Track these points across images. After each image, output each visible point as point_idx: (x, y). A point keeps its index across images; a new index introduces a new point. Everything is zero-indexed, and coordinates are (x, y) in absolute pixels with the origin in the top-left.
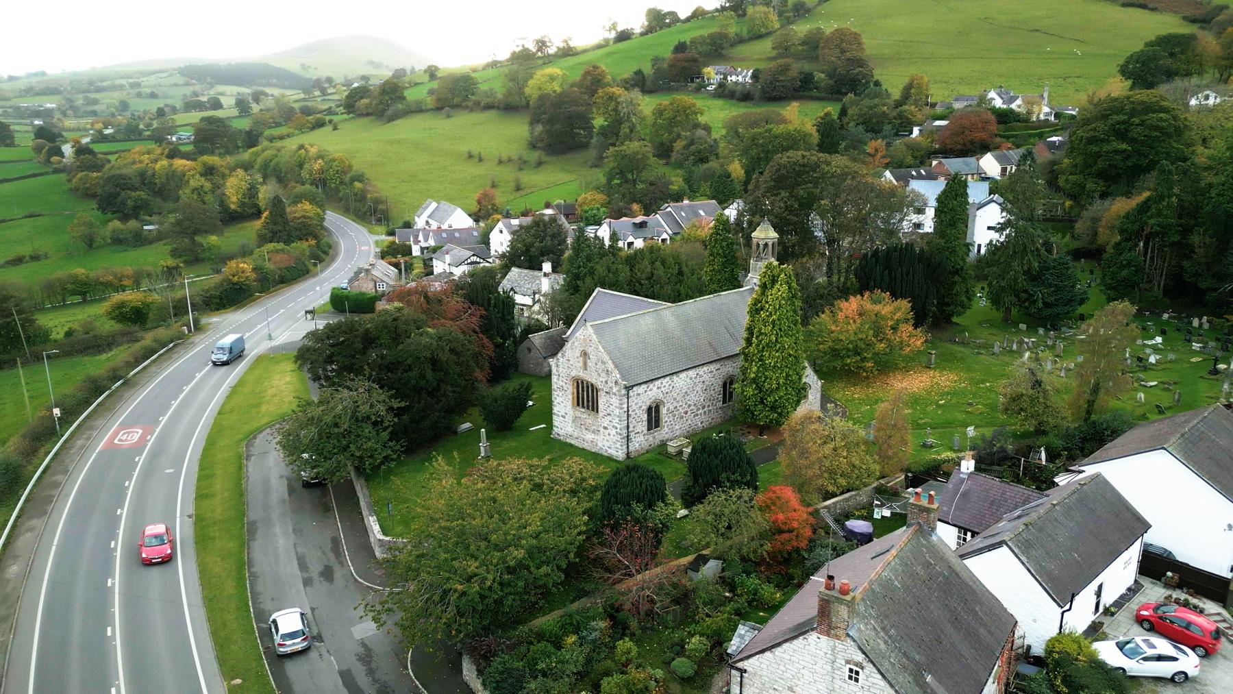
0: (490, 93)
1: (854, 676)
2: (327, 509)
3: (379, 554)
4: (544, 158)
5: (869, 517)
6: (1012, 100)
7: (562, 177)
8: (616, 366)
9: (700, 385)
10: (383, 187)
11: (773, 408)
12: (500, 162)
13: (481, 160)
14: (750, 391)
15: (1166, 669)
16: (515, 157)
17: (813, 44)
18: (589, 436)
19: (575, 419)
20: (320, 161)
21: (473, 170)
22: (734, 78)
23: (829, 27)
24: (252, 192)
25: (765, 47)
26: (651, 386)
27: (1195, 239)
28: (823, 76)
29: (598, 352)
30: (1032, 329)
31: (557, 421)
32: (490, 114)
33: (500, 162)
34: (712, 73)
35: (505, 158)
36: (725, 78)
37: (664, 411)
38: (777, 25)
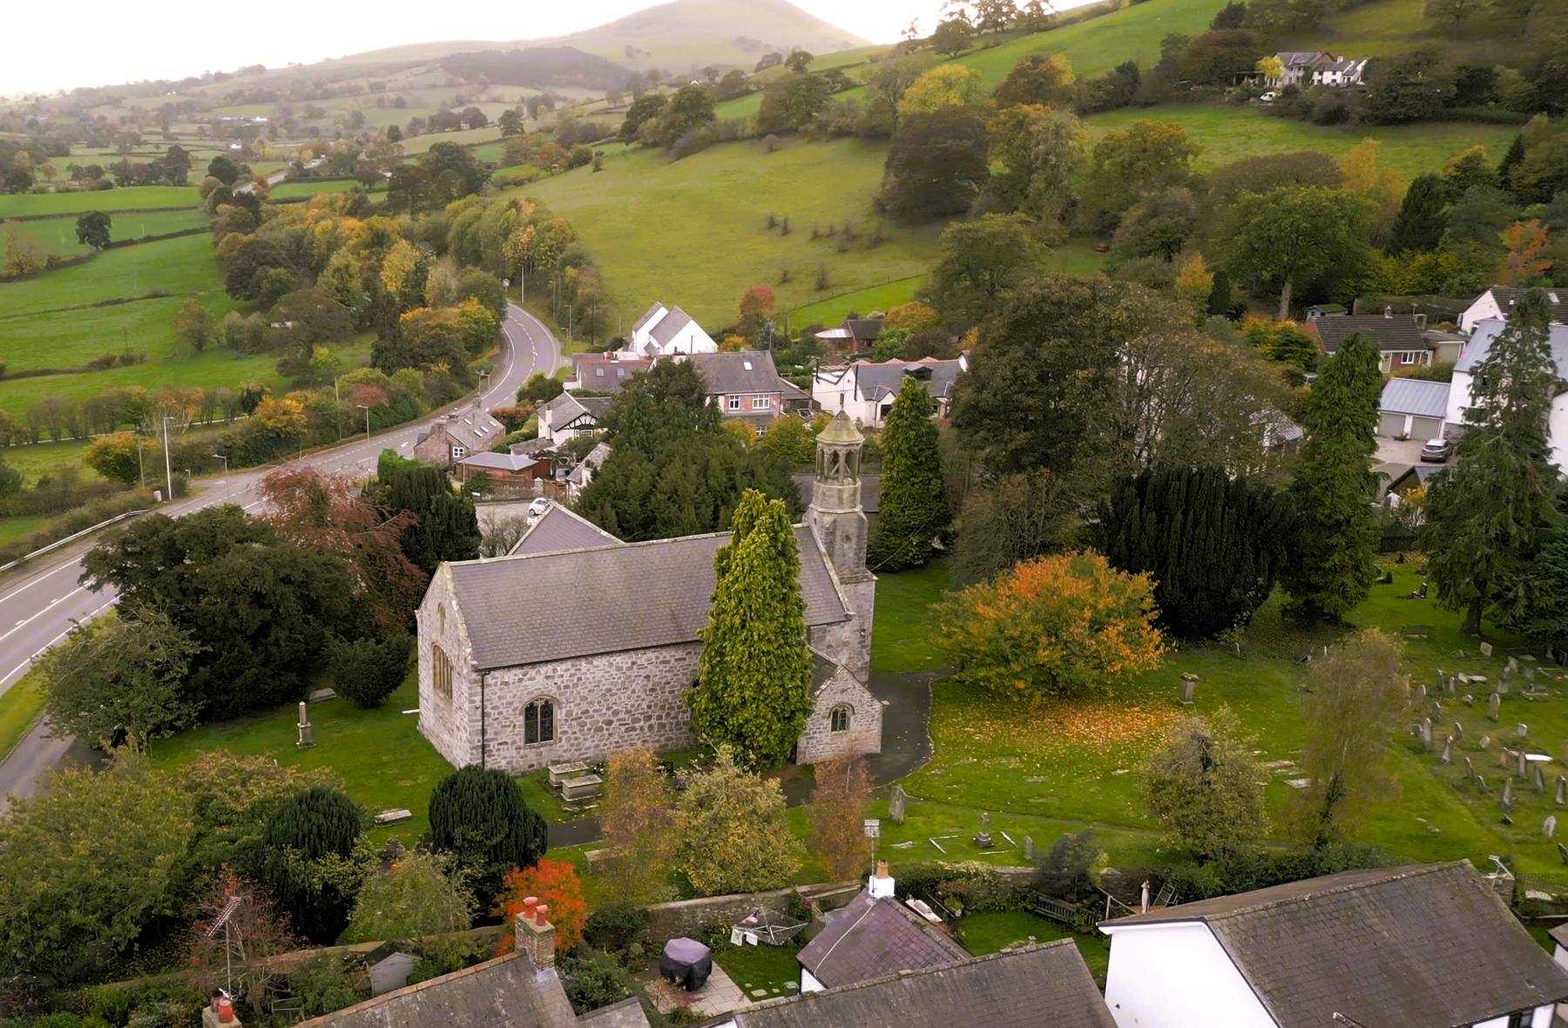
8: (471, 634)
9: (640, 681)
12: (816, 236)
16: (839, 228)
21: (774, 250)
22: (1328, 77)
26: (532, 672)
30: (1503, 650)
32: (844, 144)
33: (816, 236)
34: (1280, 70)
35: (823, 231)
36: (1307, 79)
37: (559, 715)
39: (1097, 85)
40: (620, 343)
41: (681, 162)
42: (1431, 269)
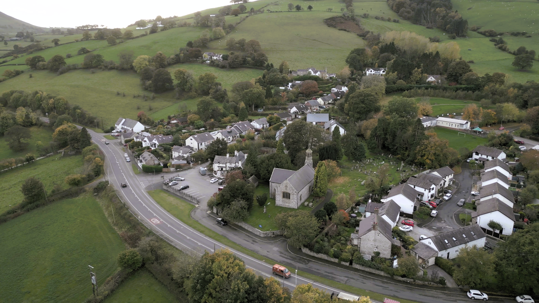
0: (111, 63)
1: (378, 235)
2: (236, 230)
3: (262, 235)
4: (155, 95)
5: (354, 213)
6: (315, 72)
7: (165, 103)
10: (91, 112)
11: (323, 193)
12: (134, 97)
13: (124, 96)
14: (318, 189)
15: (408, 230)
17: (242, 45)
18: (287, 204)
19: (283, 201)
20: (52, 99)
22: (215, 58)
23: (248, 38)
24: (27, 116)
25: (223, 43)
27: (388, 136)
28: (250, 59)
29: (290, 185)
31: (277, 202)
36: (211, 58)
38: (224, 34)
39: (173, 59)
40: (113, 129)
41: (62, 75)
42: (273, 101)
